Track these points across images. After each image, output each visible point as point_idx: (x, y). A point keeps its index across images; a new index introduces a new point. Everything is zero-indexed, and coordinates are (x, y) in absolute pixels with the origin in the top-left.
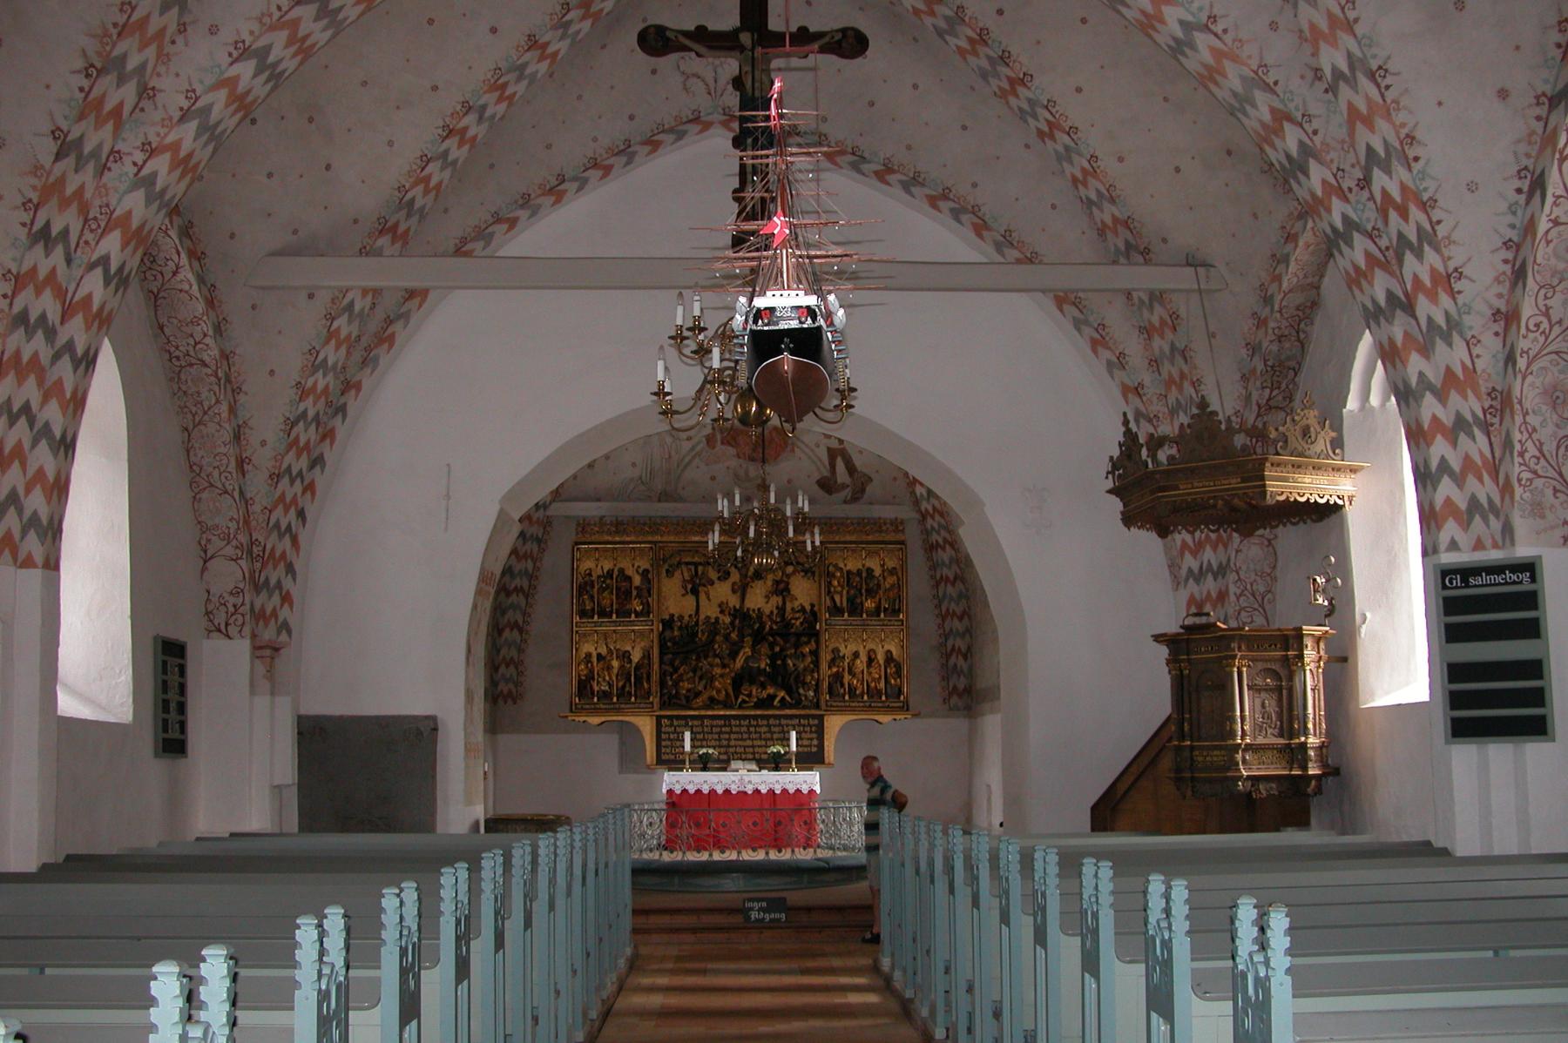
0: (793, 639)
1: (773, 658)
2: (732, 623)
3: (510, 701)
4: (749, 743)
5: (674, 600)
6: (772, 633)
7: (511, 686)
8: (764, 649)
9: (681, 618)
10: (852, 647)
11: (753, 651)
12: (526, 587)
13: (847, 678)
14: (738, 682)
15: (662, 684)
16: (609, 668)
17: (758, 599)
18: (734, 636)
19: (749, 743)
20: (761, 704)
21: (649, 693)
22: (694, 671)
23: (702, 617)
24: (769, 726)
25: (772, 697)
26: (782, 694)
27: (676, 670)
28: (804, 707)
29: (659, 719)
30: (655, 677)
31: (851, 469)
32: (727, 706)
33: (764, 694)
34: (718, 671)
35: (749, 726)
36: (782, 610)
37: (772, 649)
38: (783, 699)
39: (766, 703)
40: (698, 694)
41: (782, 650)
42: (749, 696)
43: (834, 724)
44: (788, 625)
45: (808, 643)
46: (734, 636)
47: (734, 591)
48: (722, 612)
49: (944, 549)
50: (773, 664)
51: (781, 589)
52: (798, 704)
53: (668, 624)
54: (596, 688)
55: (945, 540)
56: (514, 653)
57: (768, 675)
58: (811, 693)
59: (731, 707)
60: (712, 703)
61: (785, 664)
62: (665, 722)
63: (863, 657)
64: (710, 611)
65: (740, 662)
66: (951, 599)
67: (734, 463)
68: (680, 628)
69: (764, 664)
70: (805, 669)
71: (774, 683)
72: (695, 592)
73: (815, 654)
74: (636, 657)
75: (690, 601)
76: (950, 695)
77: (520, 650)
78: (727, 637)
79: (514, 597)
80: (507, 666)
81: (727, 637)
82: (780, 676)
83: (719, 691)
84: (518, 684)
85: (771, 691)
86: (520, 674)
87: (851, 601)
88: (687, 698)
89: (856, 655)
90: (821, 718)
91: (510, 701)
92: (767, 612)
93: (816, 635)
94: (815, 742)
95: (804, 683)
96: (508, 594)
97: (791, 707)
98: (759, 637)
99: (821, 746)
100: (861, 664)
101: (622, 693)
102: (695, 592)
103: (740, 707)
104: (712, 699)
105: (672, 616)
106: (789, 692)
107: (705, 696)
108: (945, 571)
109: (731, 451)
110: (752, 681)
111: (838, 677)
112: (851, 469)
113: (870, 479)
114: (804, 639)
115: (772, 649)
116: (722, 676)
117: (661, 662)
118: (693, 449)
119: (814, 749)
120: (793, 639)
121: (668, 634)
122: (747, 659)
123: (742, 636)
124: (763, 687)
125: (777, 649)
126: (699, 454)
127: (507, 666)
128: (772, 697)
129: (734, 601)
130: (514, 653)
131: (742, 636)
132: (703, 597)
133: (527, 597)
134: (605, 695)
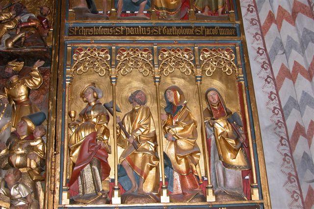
13: (116, 156)
45: (24, 75)
66: (292, 44)
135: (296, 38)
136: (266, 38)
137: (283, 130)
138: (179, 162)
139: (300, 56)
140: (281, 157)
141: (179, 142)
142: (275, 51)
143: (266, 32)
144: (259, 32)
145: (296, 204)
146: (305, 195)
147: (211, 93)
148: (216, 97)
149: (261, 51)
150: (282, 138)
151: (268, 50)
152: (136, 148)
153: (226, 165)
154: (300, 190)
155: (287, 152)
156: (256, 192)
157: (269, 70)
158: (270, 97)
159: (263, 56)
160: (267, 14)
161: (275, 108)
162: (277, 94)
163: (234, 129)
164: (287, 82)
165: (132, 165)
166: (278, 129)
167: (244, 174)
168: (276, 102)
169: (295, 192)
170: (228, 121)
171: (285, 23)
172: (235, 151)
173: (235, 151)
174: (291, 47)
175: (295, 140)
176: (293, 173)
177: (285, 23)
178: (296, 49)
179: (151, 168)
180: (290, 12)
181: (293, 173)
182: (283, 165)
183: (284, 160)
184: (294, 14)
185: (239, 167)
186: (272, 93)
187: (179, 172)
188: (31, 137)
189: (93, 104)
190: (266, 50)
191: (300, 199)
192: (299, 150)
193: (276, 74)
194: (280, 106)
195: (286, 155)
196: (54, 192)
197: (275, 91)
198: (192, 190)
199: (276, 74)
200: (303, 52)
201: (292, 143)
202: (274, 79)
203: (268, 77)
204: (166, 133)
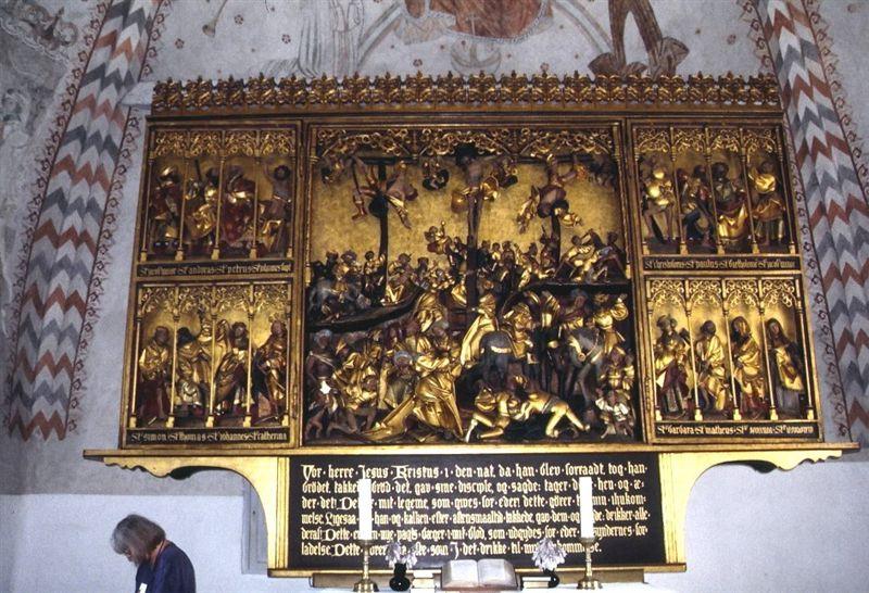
0: (580, 298)
1: (541, 336)
2: (454, 272)
3: (54, 434)
4: (497, 518)
5: (339, 232)
6: (535, 285)
7: (59, 406)
8: (521, 319)
9: (349, 257)
10: (699, 317)
11: (500, 324)
12: (94, 233)
14: (467, 388)
15: (310, 391)
16: (202, 360)
17: (505, 224)
18: (458, 294)
19: (497, 518)
20: (517, 432)
21: (279, 409)
22: (378, 367)
23: (393, 258)
24: (538, 478)
25: (541, 419)
26: (560, 411)
27: (339, 360)
28: (610, 440)
29: (296, 463)
30: (293, 376)
31: (650, 34)
32: (443, 435)
33: (524, 412)
34: (426, 363)
35: (494, 481)
36: (551, 243)
37: (537, 318)
38: (564, 421)
39: (530, 429)
40: (381, 415)
41: (558, 321)
42: (494, 415)
43: (681, 472)
44: (568, 269)
45: (611, 305)
46: (458, 294)
47: (455, 208)
48: (433, 247)
49: (827, 153)
50: (540, 350)
51: (550, 208)
52: (595, 433)
53: (324, 271)
54: (174, 400)
55: (829, 137)
56: (68, 347)
57: (531, 373)
58: (622, 410)
59: (456, 439)
60: (414, 430)
61: (565, 348)
62: (311, 470)
63: (722, 336)
64: (407, 244)
65: (468, 350)
66: (844, 244)
67: (453, 39)
68: (349, 277)
69: (522, 346)
70: (607, 360)
71: (544, 390)
72: (378, 208)
73: (627, 327)
74: (260, 337)
75: (370, 232)
76: (850, 419)
77: (80, 344)
78: (444, 297)
79: (67, 250)
80: (55, 371)
81: (444, 297)
82: (552, 369)
83: (426, 407)
84: (70, 403)
85: (539, 405)
86: (77, 384)
87: (690, 223)
88: (360, 418)
89: (707, 330)
90: (651, 461)
91: (54, 434)
92: (524, 246)
93: (628, 290)
94: (642, 515)
95: (607, 389)
96: (57, 242)
97: (583, 438)
98: (508, 296)
99: (655, 522)
100: (717, 348)
101: (230, 414)
102: (378, 208)
103: (475, 440)
104: (411, 421)
105: (333, 257)
106: (578, 407)
107: (398, 418)
108: (831, 195)
109: (448, 20)
110: (500, 384)
111: (675, 375)
112: (650, 34)
113: (685, 50)
114: (600, 298)
115: (537, 318)
116: (434, 374)
117: (308, 346)
118: (385, 16)
119: (641, 531)
120: (580, 298)
121: (325, 290)
122: (485, 341)
123: (473, 297)
124: (522, 396)
125: (548, 319)
126: (393, 27)
127: (55, 371)
128: (541, 419)
129: (457, 230)
130: (68, 347)
131: (473, 297)
132: (393, 222)
133: (95, 250)
134: (189, 417)
135: (849, 237)
136: (815, 232)
137: (829, 336)
138: (745, 385)
139: (853, 258)
140: (826, 367)
141: (745, 368)
142: (824, 249)
143: (814, 225)
144: (807, 225)
145: (840, 416)
146: (849, 408)
147: (773, 324)
148: (777, 329)
149: (808, 247)
150: (828, 345)
151: (817, 246)
152: (711, 374)
153: (785, 388)
154: (845, 402)
155: (833, 361)
156: (811, 413)
157: (817, 269)
158: (816, 299)
159: (810, 253)
160: (817, 204)
161: (821, 312)
162: (825, 297)
163: (793, 359)
164: (836, 283)
165: (707, 388)
166: (824, 336)
167: (800, 396)
168: (822, 304)
169: (839, 404)
170: (787, 350)
171: (837, 219)
172: (792, 378)
173: (792, 378)
174: (843, 247)
175: (842, 348)
176: (838, 384)
177: (837, 219)
178: (848, 249)
179: (722, 389)
180: (844, 208)
181: (838, 384)
182: (827, 375)
183: (829, 369)
184: (849, 208)
185: (797, 391)
186: (818, 295)
187: (745, 394)
188: (623, 363)
189: (670, 333)
190: (813, 245)
191: (844, 413)
192: (847, 357)
193: (824, 274)
194: (827, 309)
195: (831, 364)
196: (649, 411)
197: (821, 293)
198: (756, 410)
199: (824, 274)
200: (855, 255)
201: (838, 352)
202: (821, 280)
203: (815, 276)
204: (735, 360)
